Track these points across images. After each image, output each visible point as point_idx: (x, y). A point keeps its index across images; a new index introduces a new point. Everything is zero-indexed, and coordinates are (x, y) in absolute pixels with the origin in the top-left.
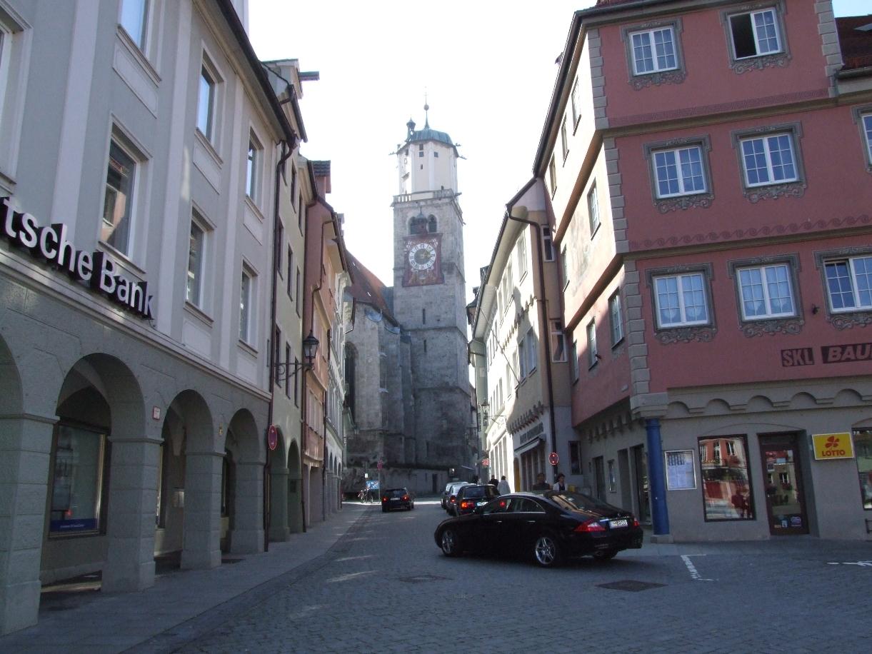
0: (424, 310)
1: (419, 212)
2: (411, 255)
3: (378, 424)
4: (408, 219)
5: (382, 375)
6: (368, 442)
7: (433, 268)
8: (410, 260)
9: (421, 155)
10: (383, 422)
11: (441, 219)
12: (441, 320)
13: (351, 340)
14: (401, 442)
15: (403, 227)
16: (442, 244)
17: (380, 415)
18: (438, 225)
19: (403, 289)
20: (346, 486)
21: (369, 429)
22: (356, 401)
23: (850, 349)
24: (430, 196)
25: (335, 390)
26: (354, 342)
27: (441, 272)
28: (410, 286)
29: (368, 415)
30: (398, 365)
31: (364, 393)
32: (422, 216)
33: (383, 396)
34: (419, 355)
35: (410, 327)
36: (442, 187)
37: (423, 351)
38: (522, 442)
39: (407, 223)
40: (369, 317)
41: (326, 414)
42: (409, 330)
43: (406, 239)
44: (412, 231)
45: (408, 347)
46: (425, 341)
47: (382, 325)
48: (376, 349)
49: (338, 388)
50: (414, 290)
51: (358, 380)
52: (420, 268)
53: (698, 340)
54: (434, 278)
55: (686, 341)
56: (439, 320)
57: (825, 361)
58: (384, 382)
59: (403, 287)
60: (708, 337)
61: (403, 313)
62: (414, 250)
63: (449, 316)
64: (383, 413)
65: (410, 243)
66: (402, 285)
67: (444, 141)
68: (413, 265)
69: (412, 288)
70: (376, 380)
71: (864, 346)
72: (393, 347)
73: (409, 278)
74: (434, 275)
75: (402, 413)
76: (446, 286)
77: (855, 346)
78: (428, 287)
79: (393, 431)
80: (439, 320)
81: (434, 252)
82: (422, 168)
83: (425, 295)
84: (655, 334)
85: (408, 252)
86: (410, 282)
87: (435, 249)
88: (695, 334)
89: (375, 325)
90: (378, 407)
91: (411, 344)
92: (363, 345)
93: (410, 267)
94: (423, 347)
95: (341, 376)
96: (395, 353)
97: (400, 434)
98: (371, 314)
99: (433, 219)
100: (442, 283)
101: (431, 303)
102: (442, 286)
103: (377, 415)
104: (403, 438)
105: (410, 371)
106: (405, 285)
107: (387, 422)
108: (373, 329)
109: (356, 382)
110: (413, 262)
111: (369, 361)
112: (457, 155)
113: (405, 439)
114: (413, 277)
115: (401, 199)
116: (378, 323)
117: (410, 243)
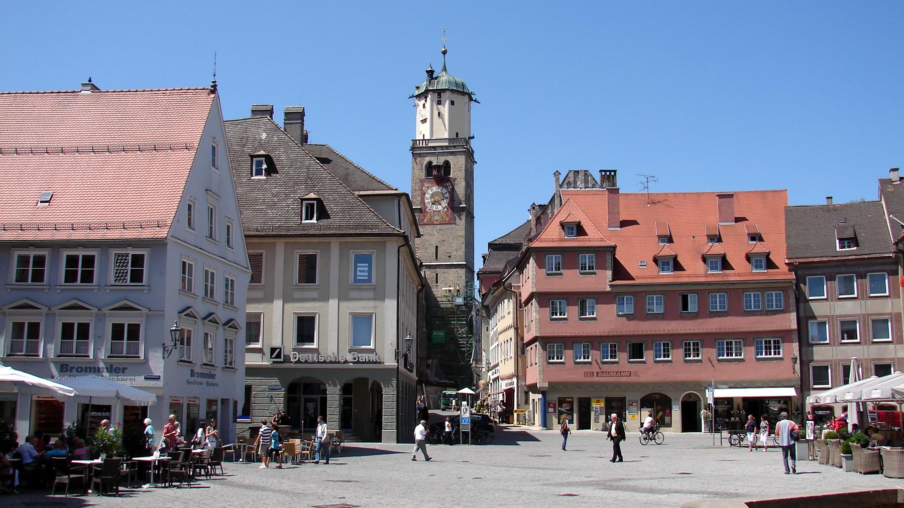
0: (437, 247)
2: (427, 196)
4: (425, 163)
8: (426, 201)
11: (455, 165)
15: (421, 169)
23: (605, 373)
39: (424, 166)
43: (422, 181)
46: (437, 275)
52: (434, 209)
54: (447, 219)
56: (450, 257)
57: (597, 376)
62: (430, 192)
65: (426, 185)
68: (429, 206)
71: (609, 372)
74: (448, 216)
76: (456, 226)
77: (606, 372)
78: (443, 227)
80: (450, 257)
85: (425, 194)
86: (425, 221)
93: (426, 207)
94: (435, 280)
100: (454, 224)
101: (443, 241)
102: (453, 226)
112: (471, 99)
114: (428, 216)
117: (426, 185)
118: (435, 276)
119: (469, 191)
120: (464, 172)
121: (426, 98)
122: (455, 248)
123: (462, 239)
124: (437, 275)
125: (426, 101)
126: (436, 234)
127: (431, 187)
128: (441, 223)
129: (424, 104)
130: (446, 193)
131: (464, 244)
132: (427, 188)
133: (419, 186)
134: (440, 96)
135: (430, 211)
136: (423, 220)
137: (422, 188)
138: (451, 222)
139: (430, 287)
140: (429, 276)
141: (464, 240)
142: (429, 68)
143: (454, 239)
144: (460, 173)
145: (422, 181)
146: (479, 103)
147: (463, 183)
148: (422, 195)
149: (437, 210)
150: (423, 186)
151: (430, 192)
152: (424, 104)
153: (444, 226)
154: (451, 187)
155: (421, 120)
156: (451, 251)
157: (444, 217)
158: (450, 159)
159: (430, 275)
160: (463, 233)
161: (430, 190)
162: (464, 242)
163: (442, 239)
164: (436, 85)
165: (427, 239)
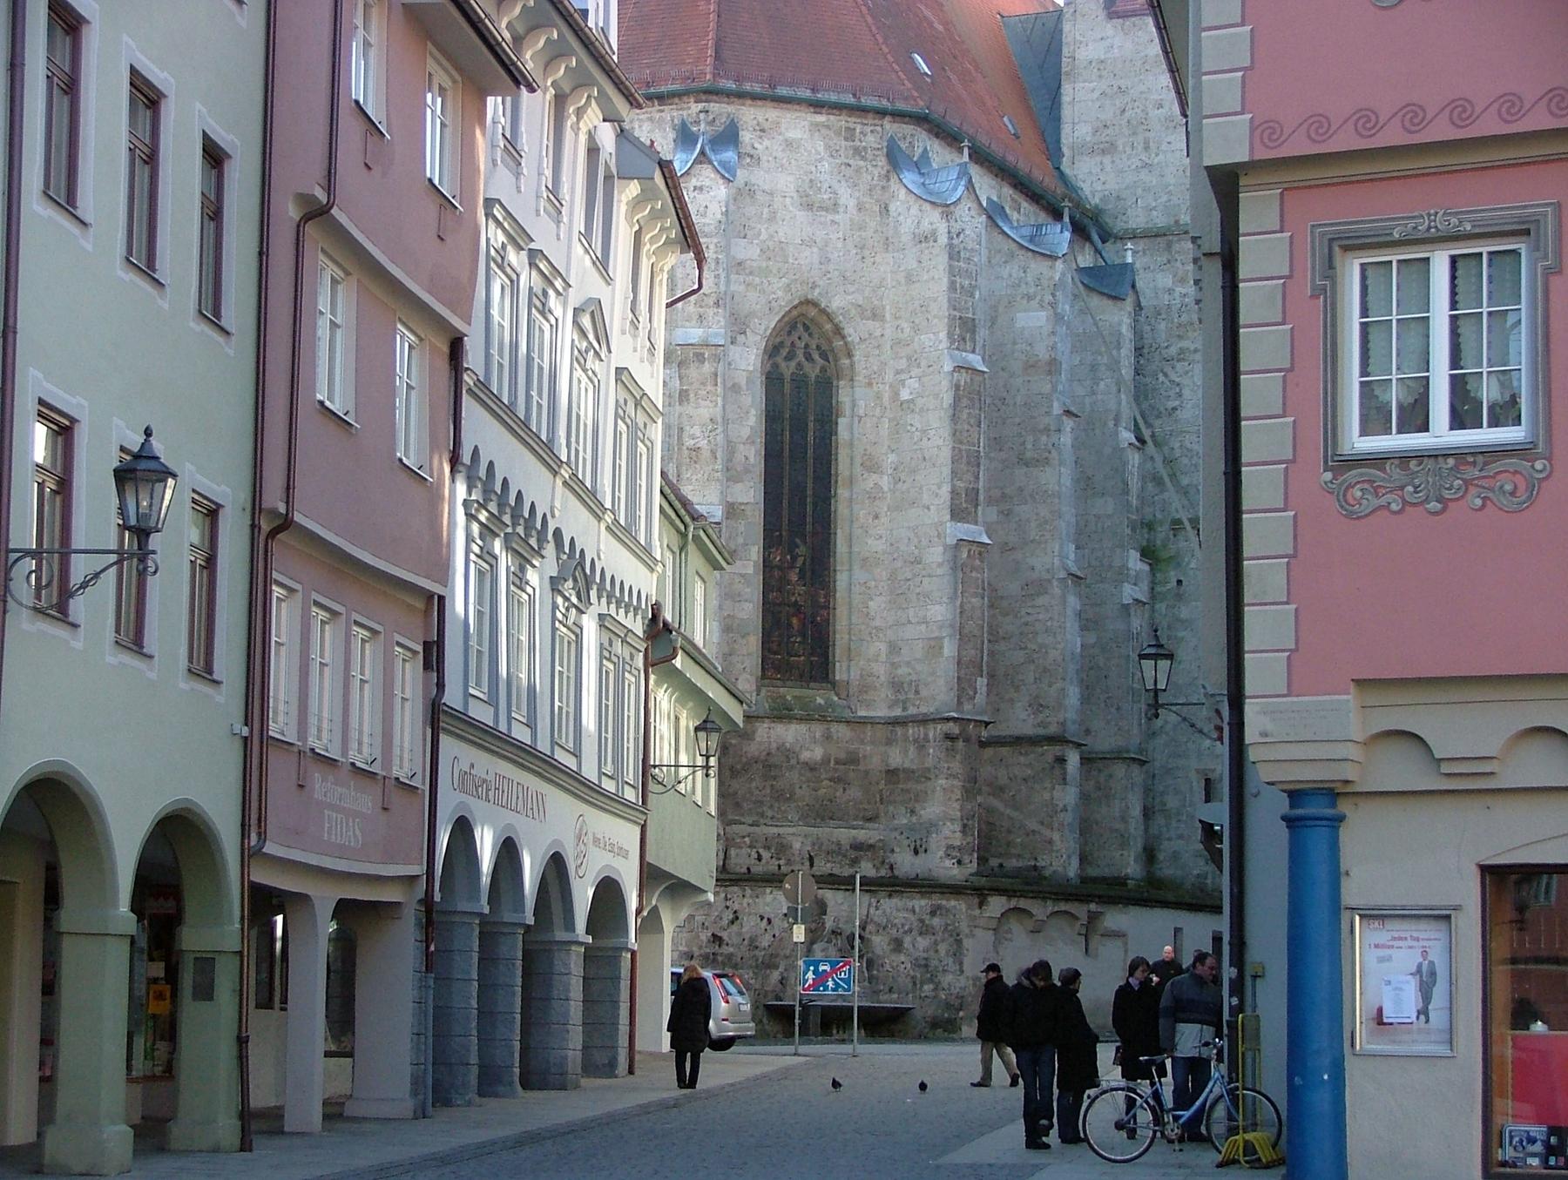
3: (938, 692)
5: (965, 459)
6: (892, 774)
10: (963, 688)
13: (815, 295)
14: (1064, 781)
17: (949, 649)
19: (1110, 29)
20: (775, 976)
21: (898, 712)
26: (836, 303)
29: (894, 648)
30: (1057, 409)
31: (875, 545)
33: (965, 557)
34: (1182, 355)
35: (1136, 219)
38: (649, 863)
40: (909, 178)
41: (441, 686)
42: (1134, 236)
45: (1118, 317)
47: (972, 222)
48: (936, 339)
51: (851, 481)
53: (1479, 502)
55: (1434, 506)
58: (973, 495)
60: (1513, 494)
61: (1109, 149)
64: (963, 638)
70: (936, 487)
72: (1033, 320)
75: (1071, 638)
79: (1020, 720)
84: (1328, 476)
88: (1467, 483)
89: (932, 219)
90: (940, 612)
91: (1139, 306)
92: (876, 315)
96: (1042, 353)
97: (1058, 740)
98: (921, 165)
103: (934, 647)
104: (1073, 758)
105: (1127, 436)
107: (982, 682)
108: (926, 238)
109: (842, 492)
111: (905, 395)
113: (1086, 760)
116: (947, 209)
159: (1170, 291)
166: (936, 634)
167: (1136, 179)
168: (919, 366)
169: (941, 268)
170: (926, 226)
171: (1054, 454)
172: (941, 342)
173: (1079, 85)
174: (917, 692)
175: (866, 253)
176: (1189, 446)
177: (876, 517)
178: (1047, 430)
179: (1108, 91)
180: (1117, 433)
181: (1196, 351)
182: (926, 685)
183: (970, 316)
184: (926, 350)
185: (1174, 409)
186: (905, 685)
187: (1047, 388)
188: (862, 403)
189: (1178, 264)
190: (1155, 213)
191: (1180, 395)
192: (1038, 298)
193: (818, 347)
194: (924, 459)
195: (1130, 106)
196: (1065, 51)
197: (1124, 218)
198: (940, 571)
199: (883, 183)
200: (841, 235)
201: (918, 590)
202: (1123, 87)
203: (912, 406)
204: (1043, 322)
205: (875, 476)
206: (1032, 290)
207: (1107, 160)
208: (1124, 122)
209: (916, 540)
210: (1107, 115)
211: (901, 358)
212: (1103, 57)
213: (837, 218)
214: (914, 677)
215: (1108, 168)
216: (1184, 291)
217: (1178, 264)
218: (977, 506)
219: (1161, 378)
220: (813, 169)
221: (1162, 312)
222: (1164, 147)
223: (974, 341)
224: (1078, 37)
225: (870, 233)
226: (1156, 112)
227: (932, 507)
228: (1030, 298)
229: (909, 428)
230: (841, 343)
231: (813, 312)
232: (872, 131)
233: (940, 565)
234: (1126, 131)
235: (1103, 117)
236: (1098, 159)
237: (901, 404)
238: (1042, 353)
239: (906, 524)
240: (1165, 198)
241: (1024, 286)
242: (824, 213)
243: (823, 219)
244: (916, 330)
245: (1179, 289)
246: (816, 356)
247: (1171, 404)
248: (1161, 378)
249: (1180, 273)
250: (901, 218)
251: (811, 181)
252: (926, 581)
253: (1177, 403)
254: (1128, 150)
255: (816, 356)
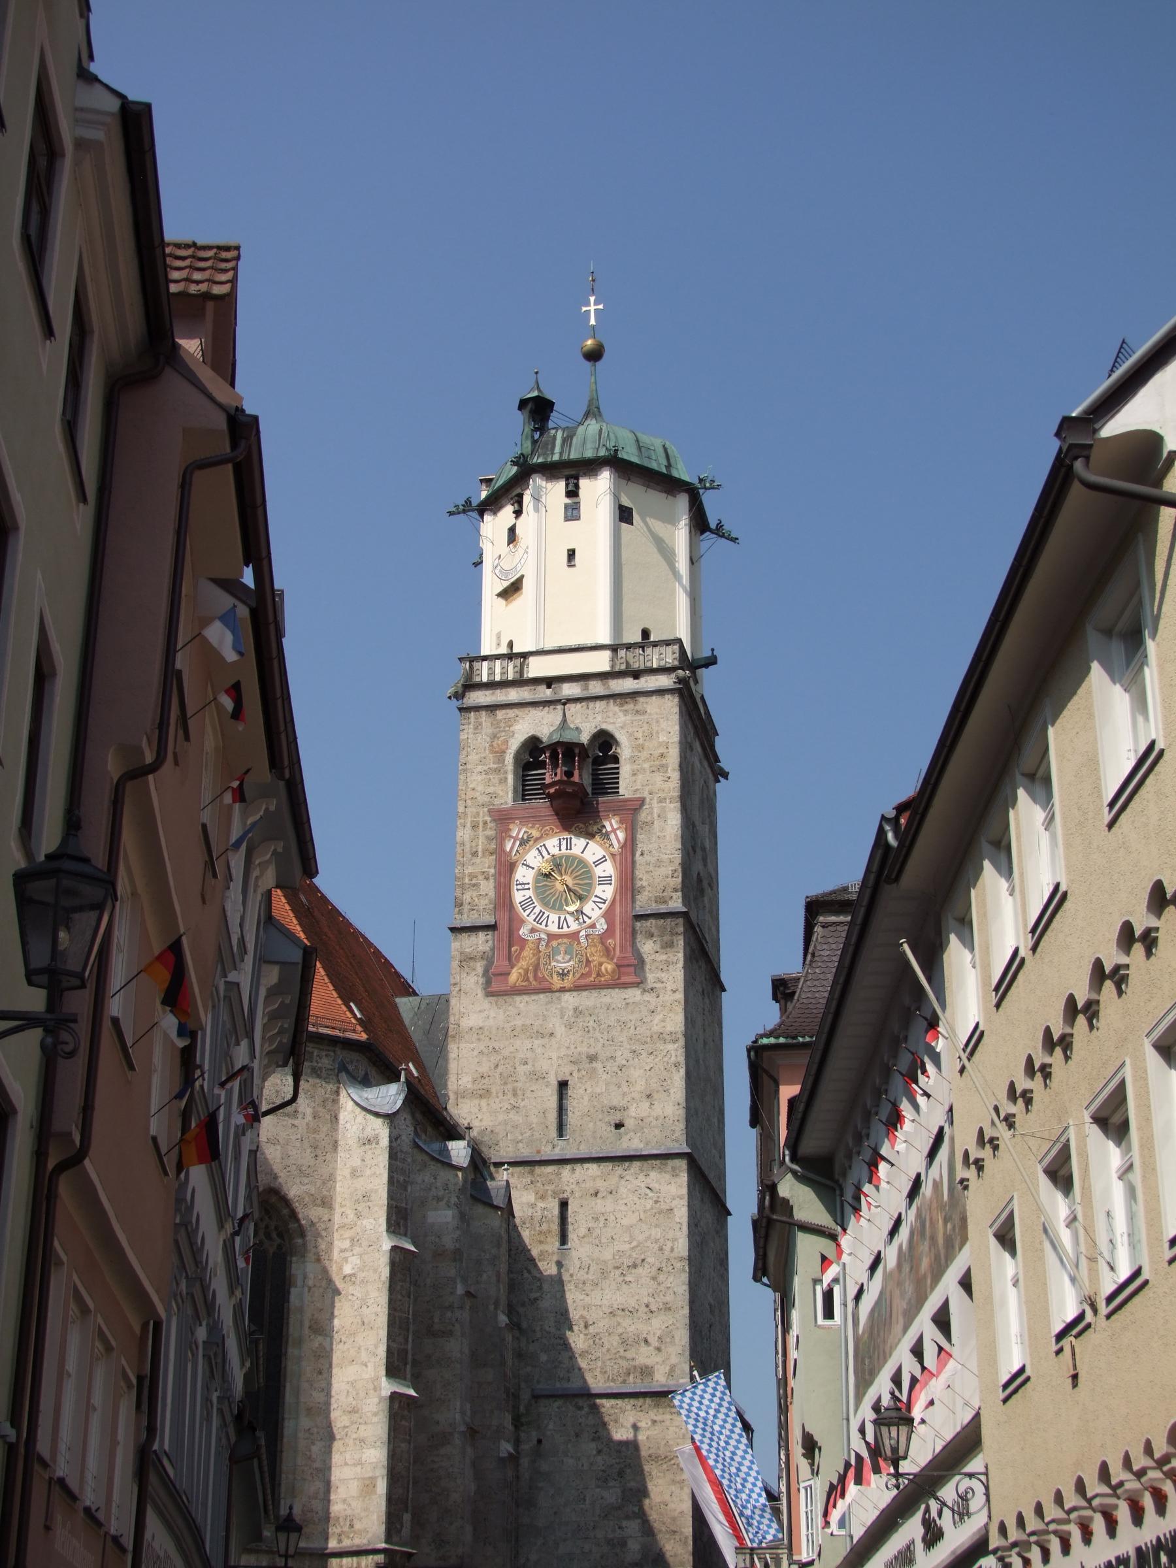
0: (563, 1085)
1: (560, 718)
2: (523, 875)
4: (515, 744)
7: (602, 926)
8: (518, 897)
9: (572, 513)
11: (640, 748)
12: (629, 1123)
15: (497, 771)
16: (640, 837)
18: (625, 770)
19: (485, 1003)
22: (289, 1426)
24: (601, 662)
25: (201, 1333)
27: (633, 944)
28: (517, 991)
30: (460, 1290)
32: (568, 737)
36: (645, 633)
37: (553, 1244)
39: (509, 759)
41: (151, 1430)
43: (502, 819)
44: (524, 791)
46: (564, 1205)
49: (215, 1329)
50: (528, 1007)
51: (299, 1342)
52: (553, 928)
54: (608, 967)
56: (619, 1126)
59: (489, 994)
61: (485, 1094)
62: (534, 859)
63: (658, 1110)
65: (518, 831)
66: (488, 983)
67: (654, 465)
68: (529, 918)
69: (521, 1002)
73: (511, 960)
74: (608, 952)
76: (647, 997)
80: (619, 1126)
81: (608, 869)
82: (571, 554)
83: (570, 1026)
85: (511, 867)
86: (514, 976)
87: (613, 855)
93: (515, 921)
94: (555, 1227)
95: (234, 1281)
96: (448, 1242)
99: (605, 741)
100: (637, 985)
101: (592, 1058)
102: (634, 994)
105: (503, 1319)
106: (495, 987)
107: (407, 1517)
109: (292, 1351)
110: (525, 904)
114: (526, 959)
115: (491, 672)
118: (556, 1211)
119: (698, 866)
120: (675, 776)
121: (519, 500)
122: (640, 1086)
123: (671, 1047)
124: (564, 1205)
125: (518, 513)
126: (560, 1030)
127: (537, 839)
128: (583, 982)
129: (512, 530)
130: (603, 860)
131: (682, 1071)
132: (523, 842)
133: (490, 839)
134: (577, 486)
135: (536, 936)
136: (509, 974)
137: (501, 846)
138: (625, 979)
139: (532, 1260)
140: (529, 1212)
141: (681, 1052)
142: (532, 390)
143: (638, 1047)
144: (658, 778)
145: (502, 819)
146: (735, 540)
147: (674, 819)
148: (499, 873)
149: (565, 929)
150: (502, 833)
151: (534, 859)
152: (512, 530)
153: (595, 993)
154: (621, 835)
155: (500, 589)
156: (623, 1103)
157: (596, 959)
158: (614, 720)
159: (533, 1206)
160: (675, 1021)
161: (534, 852)
162: (682, 1059)
163: (583, 1049)
164: (557, 449)
165: (521, 1055)
166: (370, 1474)
167: (506, 1118)
168: (360, 1246)
169: (382, 1165)
170: (369, 1132)
171: (457, 1326)
172: (380, 1225)
173: (462, 1045)
174: (351, 1526)
175: (319, 1152)
176: (547, 1329)
177: (320, 1373)
178: (451, 1307)
179: (485, 1051)
180: (496, 1316)
181: (553, 1253)
182: (360, 1519)
183: (404, 1205)
184: (368, 1232)
185: (536, 1299)
186: (341, 1520)
187: (452, 1273)
188: (311, 1276)
189: (539, 1185)
190: (521, 1145)
191: (540, 1288)
192: (446, 1199)
193: (276, 1228)
194: (363, 1323)
195: (502, 1062)
196: (452, 1019)
197: (497, 1148)
198: (375, 1419)
199: (334, 1097)
200: (299, 1136)
201: (354, 1436)
202: (497, 1048)
203: (353, 1279)
204: (449, 1219)
205: (320, 1338)
206: (441, 1193)
207: (484, 1102)
208: (497, 1075)
209: (355, 1393)
210: (484, 1068)
211: (345, 1239)
212: (481, 1025)
213: (296, 1122)
214: (349, 1512)
215: (484, 1109)
216: (543, 1206)
217: (539, 1185)
218: (406, 1364)
219: (526, 1275)
220: (279, 1082)
221: (527, 1222)
222: (528, 1094)
223: (406, 1227)
224: (462, 1010)
225: (322, 1135)
226: (523, 1067)
227: (369, 1364)
228: (439, 1199)
229: (350, 1297)
230: (296, 1225)
231: (274, 1199)
232: (326, 1055)
233: (375, 1414)
234: (498, 1081)
235: (481, 1070)
236: (476, 1102)
237: (345, 1277)
238: (448, 1242)
239: (345, 1379)
240: (529, 1133)
241: (434, 1190)
242: (287, 1118)
243: (285, 1123)
244: (359, 1216)
245: (541, 1204)
246: (274, 1235)
247: (533, 1295)
248: (526, 1275)
249: (541, 1193)
250: (348, 1126)
251: (277, 1091)
252: (362, 1428)
253: (538, 1294)
254: (500, 1095)
255: (274, 1235)
